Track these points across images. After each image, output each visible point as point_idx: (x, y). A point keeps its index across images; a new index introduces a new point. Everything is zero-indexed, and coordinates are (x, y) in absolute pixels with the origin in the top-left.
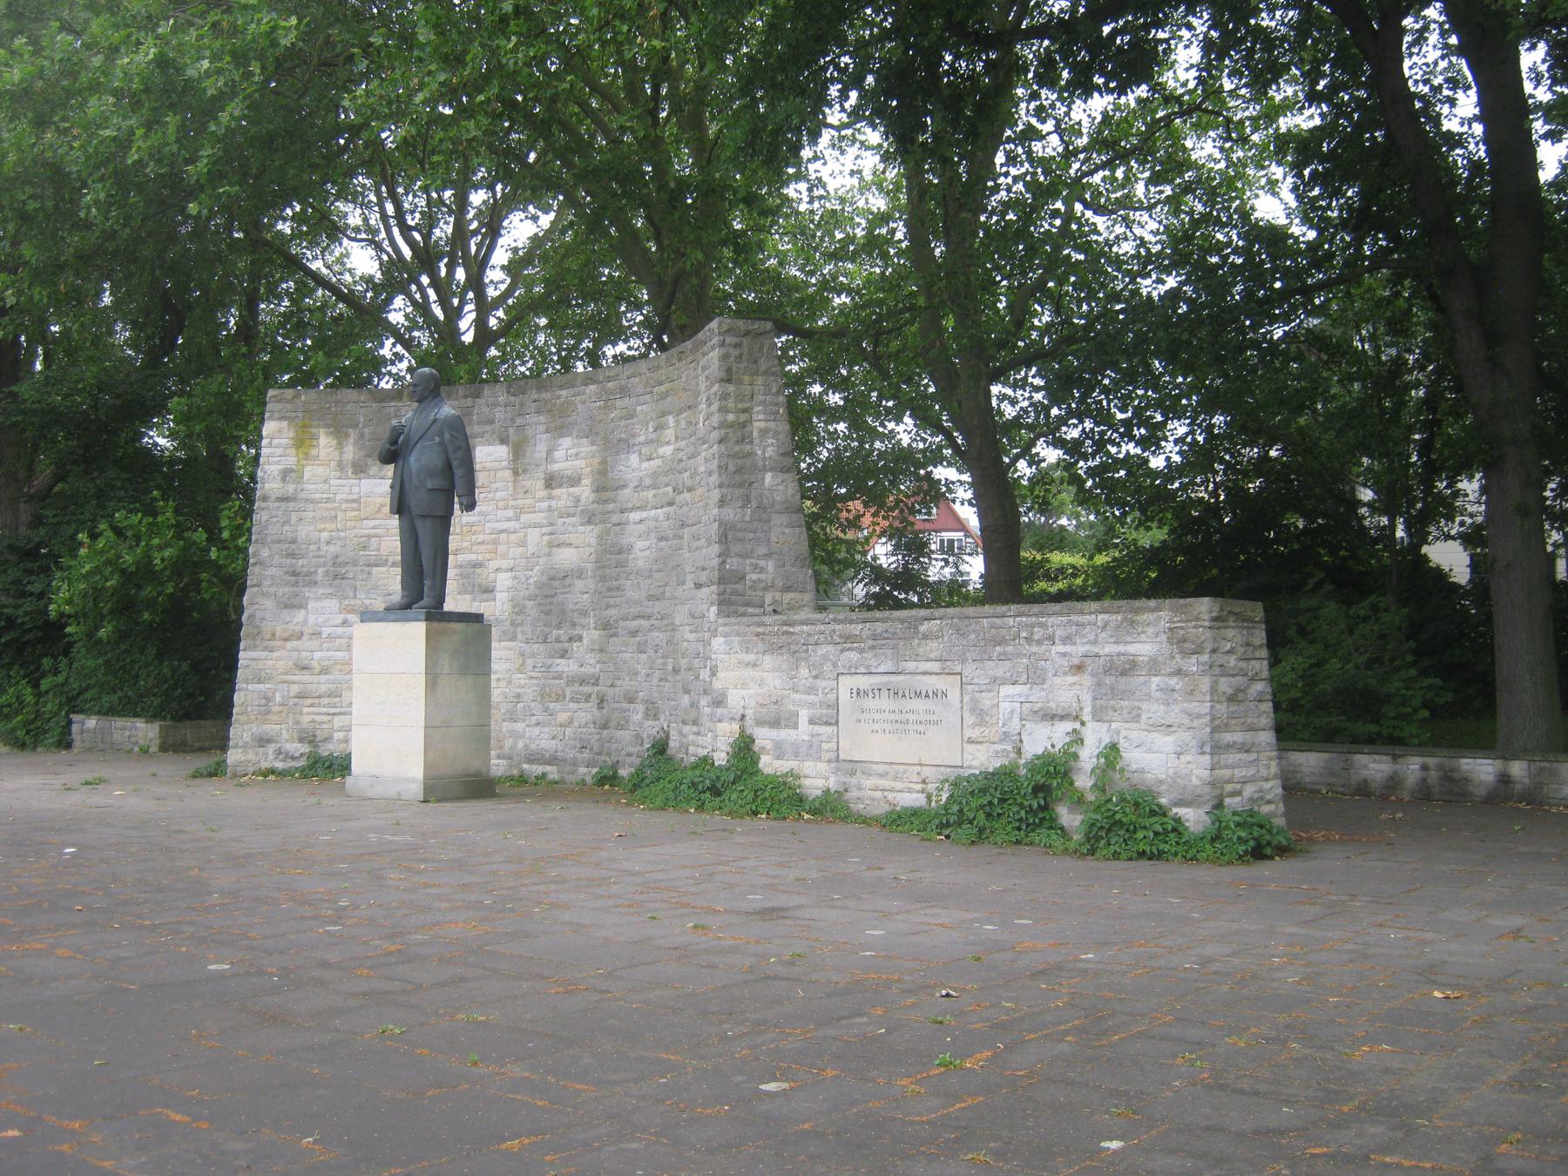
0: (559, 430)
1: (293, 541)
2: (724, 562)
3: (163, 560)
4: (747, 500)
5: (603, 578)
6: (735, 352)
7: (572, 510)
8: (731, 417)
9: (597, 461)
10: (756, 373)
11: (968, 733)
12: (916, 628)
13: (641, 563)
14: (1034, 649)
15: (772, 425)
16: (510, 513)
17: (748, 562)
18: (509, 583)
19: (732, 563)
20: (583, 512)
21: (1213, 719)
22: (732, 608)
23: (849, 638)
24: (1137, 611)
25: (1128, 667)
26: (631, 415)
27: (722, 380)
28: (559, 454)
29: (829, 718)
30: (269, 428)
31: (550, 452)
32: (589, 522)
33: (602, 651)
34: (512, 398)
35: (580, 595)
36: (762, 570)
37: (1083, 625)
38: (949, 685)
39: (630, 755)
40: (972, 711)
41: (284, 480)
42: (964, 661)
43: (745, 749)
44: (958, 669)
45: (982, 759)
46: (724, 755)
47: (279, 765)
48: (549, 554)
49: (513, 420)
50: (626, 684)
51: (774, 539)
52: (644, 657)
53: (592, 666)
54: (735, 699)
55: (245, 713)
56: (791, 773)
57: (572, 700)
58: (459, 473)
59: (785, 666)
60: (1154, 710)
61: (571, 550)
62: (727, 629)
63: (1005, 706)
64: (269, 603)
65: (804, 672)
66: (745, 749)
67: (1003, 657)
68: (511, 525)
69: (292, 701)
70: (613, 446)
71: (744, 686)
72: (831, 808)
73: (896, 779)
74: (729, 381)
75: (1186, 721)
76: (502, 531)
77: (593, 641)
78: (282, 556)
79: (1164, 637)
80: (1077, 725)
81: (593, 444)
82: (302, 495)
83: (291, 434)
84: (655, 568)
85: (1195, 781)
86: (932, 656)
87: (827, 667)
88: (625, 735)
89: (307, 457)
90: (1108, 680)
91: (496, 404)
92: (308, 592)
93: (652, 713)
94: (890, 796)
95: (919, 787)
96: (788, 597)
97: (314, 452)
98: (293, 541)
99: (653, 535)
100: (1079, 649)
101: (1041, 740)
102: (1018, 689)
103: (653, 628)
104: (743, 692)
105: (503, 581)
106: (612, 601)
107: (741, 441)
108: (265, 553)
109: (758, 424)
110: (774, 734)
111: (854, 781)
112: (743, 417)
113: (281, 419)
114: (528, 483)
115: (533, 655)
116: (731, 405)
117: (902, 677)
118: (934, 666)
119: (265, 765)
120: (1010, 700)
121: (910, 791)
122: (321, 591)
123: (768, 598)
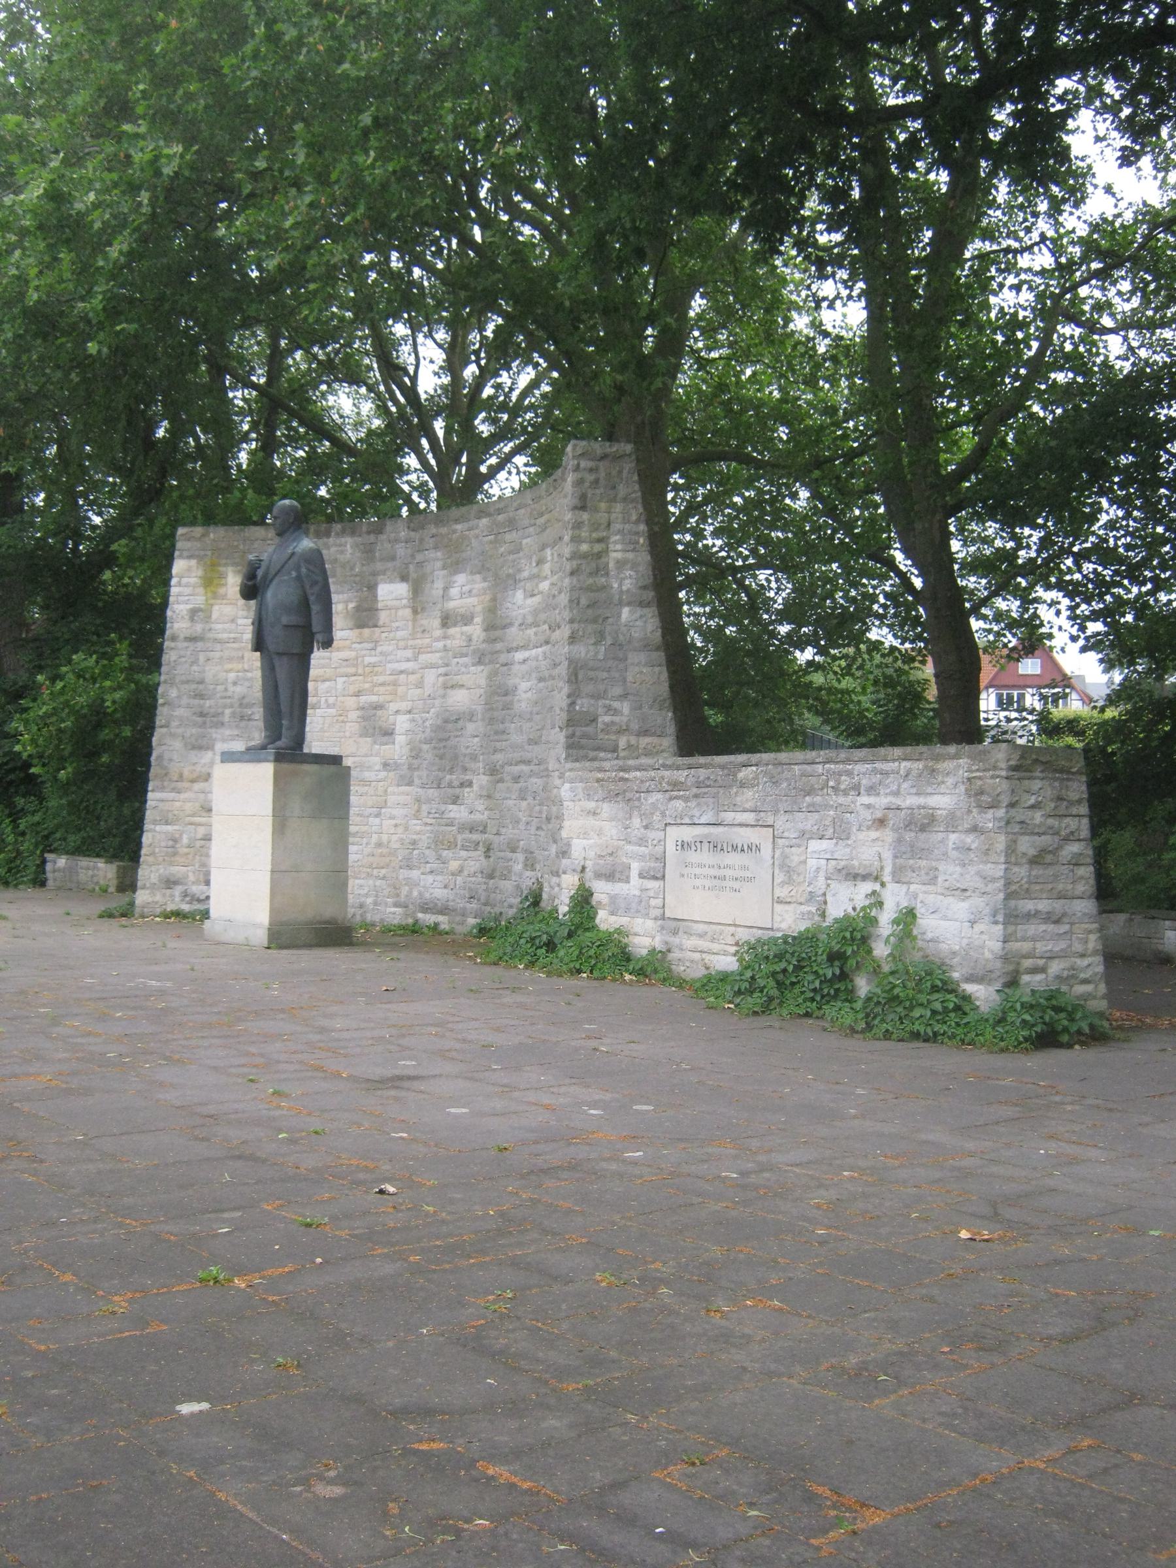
0: (455, 566)
1: (201, 682)
2: (573, 703)
3: (114, 702)
4: (601, 636)
5: (492, 721)
6: (590, 478)
8: (584, 547)
9: (488, 597)
10: (613, 500)
11: (778, 892)
12: (735, 775)
14: (841, 799)
15: (630, 555)
17: (600, 703)
18: (407, 726)
19: (583, 704)
20: (474, 652)
21: (1008, 884)
22: (582, 753)
23: (676, 785)
24: (938, 758)
25: (924, 822)
26: (518, 549)
27: (575, 508)
28: (454, 591)
30: (178, 566)
33: (489, 797)
35: (471, 738)
36: (616, 712)
37: (886, 774)
39: (511, 906)
40: (781, 867)
41: (192, 619)
43: (583, 901)
45: (790, 921)
47: (186, 907)
48: (444, 696)
49: (413, 556)
50: (509, 832)
51: (630, 678)
52: (524, 804)
54: (578, 848)
55: (153, 854)
56: (619, 931)
57: (464, 848)
58: (315, 608)
59: (621, 815)
60: (950, 872)
63: (812, 863)
64: (178, 744)
65: (636, 822)
66: (583, 901)
67: (813, 809)
68: (410, 666)
69: (199, 844)
70: (502, 582)
71: (585, 835)
72: (652, 970)
73: (713, 940)
74: (583, 508)
75: (979, 883)
76: (402, 672)
77: (481, 787)
78: (190, 697)
79: (962, 788)
80: (877, 887)
81: (485, 580)
82: (210, 635)
83: (200, 573)
84: (535, 709)
85: (988, 955)
87: (657, 817)
88: (508, 886)
89: (215, 596)
90: (909, 836)
91: (397, 541)
92: (215, 733)
96: (645, 741)
97: (222, 591)
98: (201, 682)
99: (534, 675)
100: (882, 801)
101: (844, 901)
102: (825, 844)
103: (532, 774)
105: (402, 723)
106: (498, 745)
107: (596, 572)
108: (173, 693)
109: (616, 552)
111: (675, 940)
112: (598, 547)
113: (190, 557)
114: (424, 622)
116: (584, 534)
117: (721, 829)
118: (749, 817)
119: (171, 907)
120: (818, 853)
121: (725, 953)
122: (228, 732)
123: (622, 742)
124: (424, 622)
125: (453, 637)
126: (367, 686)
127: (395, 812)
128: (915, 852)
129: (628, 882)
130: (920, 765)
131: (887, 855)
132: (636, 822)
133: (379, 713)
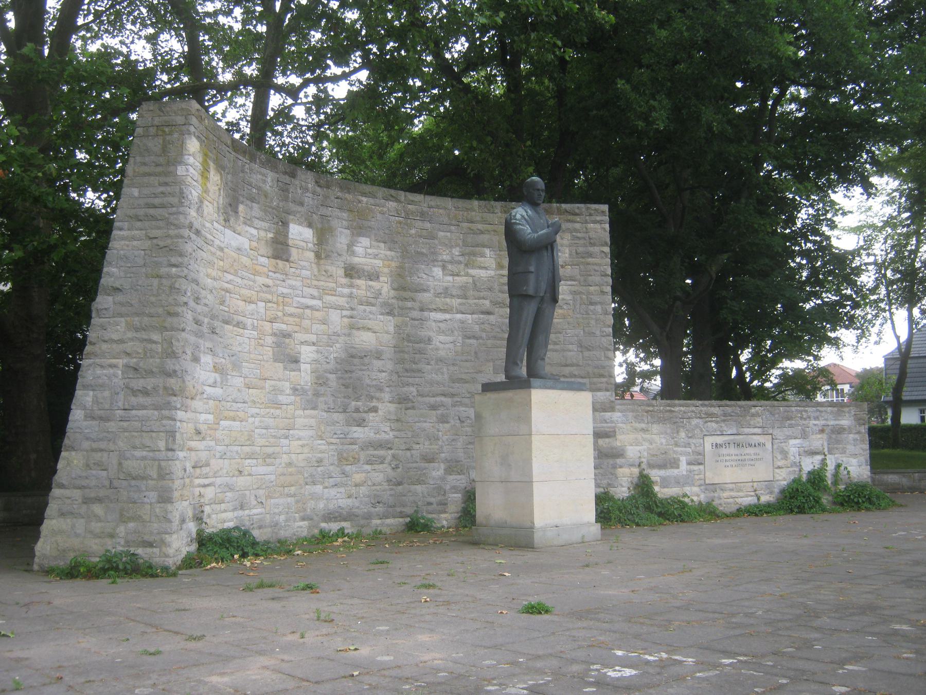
0: (359, 230)
5: (401, 361)
7: (373, 300)
9: (394, 264)
13: (442, 353)
16: (315, 292)
18: (314, 356)
23: (711, 415)
25: (839, 430)
28: (359, 250)
29: (698, 460)
31: (350, 246)
32: (389, 314)
34: (318, 189)
38: (766, 440)
39: (430, 504)
42: (773, 428)
44: (771, 432)
46: (625, 489)
50: (425, 447)
53: (387, 434)
54: (632, 452)
57: (369, 463)
59: (669, 431)
60: (851, 448)
61: (370, 334)
62: (623, 407)
65: (683, 434)
67: (791, 426)
72: (708, 512)
76: (308, 307)
80: (823, 457)
81: (390, 250)
87: (697, 431)
90: (834, 436)
93: (454, 467)
94: (739, 500)
95: (753, 494)
101: (809, 464)
102: (797, 441)
104: (638, 448)
105: (307, 353)
106: (410, 380)
110: (662, 473)
111: (716, 495)
114: (329, 268)
115: (334, 423)
117: (741, 437)
120: (794, 446)
124: (329, 268)
126: (280, 314)
127: (302, 434)
128: (838, 442)
129: (678, 467)
130: (836, 409)
131: (826, 444)
132: (683, 434)
133: (287, 341)
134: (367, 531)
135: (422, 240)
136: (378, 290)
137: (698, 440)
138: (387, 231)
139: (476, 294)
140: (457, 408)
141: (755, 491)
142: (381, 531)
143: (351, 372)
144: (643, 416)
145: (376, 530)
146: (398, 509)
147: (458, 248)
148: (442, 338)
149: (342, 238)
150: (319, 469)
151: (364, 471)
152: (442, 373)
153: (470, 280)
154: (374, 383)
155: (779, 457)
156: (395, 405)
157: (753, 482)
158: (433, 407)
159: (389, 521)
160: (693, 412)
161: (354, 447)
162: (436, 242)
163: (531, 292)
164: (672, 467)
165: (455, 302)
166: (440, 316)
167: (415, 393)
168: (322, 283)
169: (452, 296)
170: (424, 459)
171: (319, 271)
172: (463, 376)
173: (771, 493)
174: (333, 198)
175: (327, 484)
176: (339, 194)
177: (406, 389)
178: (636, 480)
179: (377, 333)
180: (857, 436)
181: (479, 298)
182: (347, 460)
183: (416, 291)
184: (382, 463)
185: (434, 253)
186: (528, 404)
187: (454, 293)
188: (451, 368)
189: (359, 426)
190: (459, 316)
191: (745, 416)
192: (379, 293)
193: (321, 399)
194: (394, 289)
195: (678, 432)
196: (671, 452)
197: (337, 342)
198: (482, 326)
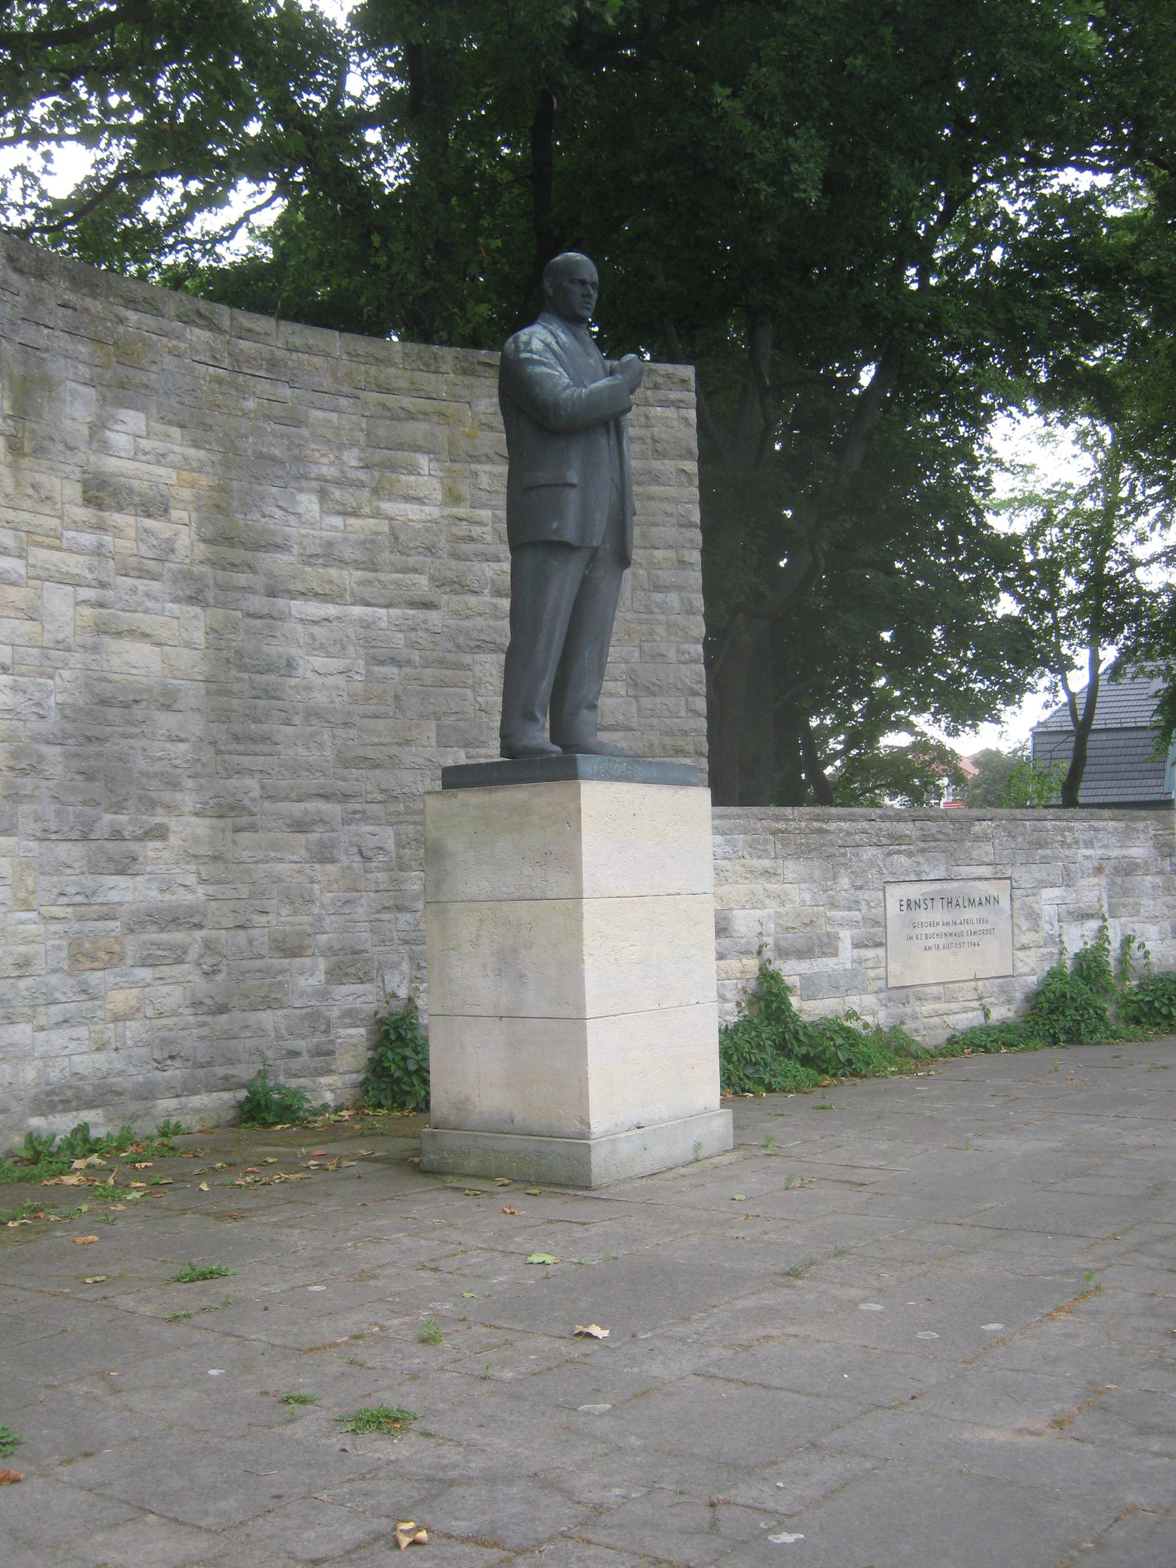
0: (119, 388)
5: (223, 716)
7: (153, 566)
9: (204, 481)
13: (320, 698)
14: (1067, 852)
23: (897, 839)
24: (1133, 820)
25: (1128, 869)
28: (119, 439)
31: (98, 428)
32: (193, 600)
44: (1008, 873)
50: (282, 919)
52: (331, 868)
57: (146, 962)
59: (817, 875)
60: (1148, 905)
61: (147, 648)
65: (844, 882)
67: (1045, 861)
72: (897, 1051)
79: (1151, 842)
81: (196, 444)
86: (986, 860)
90: (1119, 880)
93: (348, 965)
94: (951, 1020)
95: (976, 1004)
101: (1077, 938)
102: (1056, 892)
104: (757, 914)
106: (246, 761)
110: (804, 966)
117: (955, 884)
120: (1049, 900)
121: (965, 1010)
125: (118, 532)
128: (1126, 892)
130: (1122, 824)
131: (1104, 896)
132: (844, 882)
134: (147, 1127)
135: (270, 427)
136: (167, 541)
137: (873, 894)
138: (187, 400)
139: (398, 559)
140: (353, 827)
141: (980, 998)
142: (178, 1126)
143: (101, 740)
144: (766, 841)
145: (167, 1124)
146: (220, 1071)
147: (355, 451)
148: (319, 661)
149: (76, 408)
150: (22, 984)
151: (134, 984)
152: (321, 746)
153: (385, 527)
154: (158, 767)
155: (1025, 925)
156: (207, 821)
157: (976, 979)
158: (300, 826)
159: (197, 1101)
160: (864, 832)
161: (111, 924)
162: (305, 432)
163: (570, 534)
164: (824, 954)
165: (350, 578)
166: (314, 609)
167: (256, 793)
168: (26, 516)
169: (343, 563)
170: (278, 948)
171: (18, 484)
172: (370, 752)
173: (1009, 1001)
174: (52, 304)
175: (42, 1020)
176: (69, 296)
177: (234, 782)
178: (752, 986)
179: (164, 647)
180: (1158, 880)
181: (406, 570)
182: (93, 959)
183: (259, 548)
184: (179, 961)
185: (300, 460)
186: (572, 820)
187: (348, 554)
188: (340, 732)
189: (119, 873)
190: (358, 611)
191: (962, 840)
192: (167, 550)
193: (25, 808)
194: (204, 541)
195: (835, 877)
196: (822, 920)
197: (65, 666)
198: (412, 636)
